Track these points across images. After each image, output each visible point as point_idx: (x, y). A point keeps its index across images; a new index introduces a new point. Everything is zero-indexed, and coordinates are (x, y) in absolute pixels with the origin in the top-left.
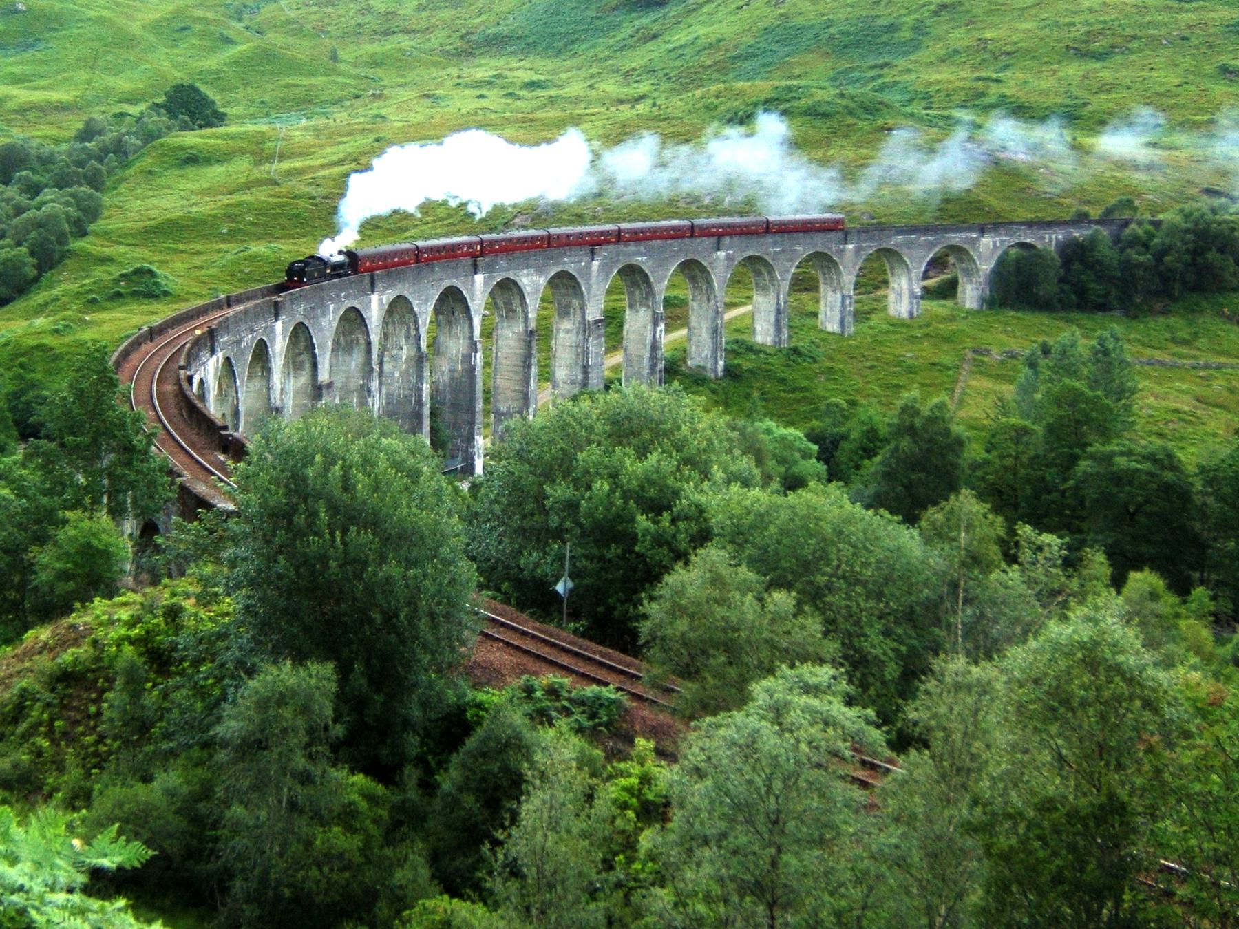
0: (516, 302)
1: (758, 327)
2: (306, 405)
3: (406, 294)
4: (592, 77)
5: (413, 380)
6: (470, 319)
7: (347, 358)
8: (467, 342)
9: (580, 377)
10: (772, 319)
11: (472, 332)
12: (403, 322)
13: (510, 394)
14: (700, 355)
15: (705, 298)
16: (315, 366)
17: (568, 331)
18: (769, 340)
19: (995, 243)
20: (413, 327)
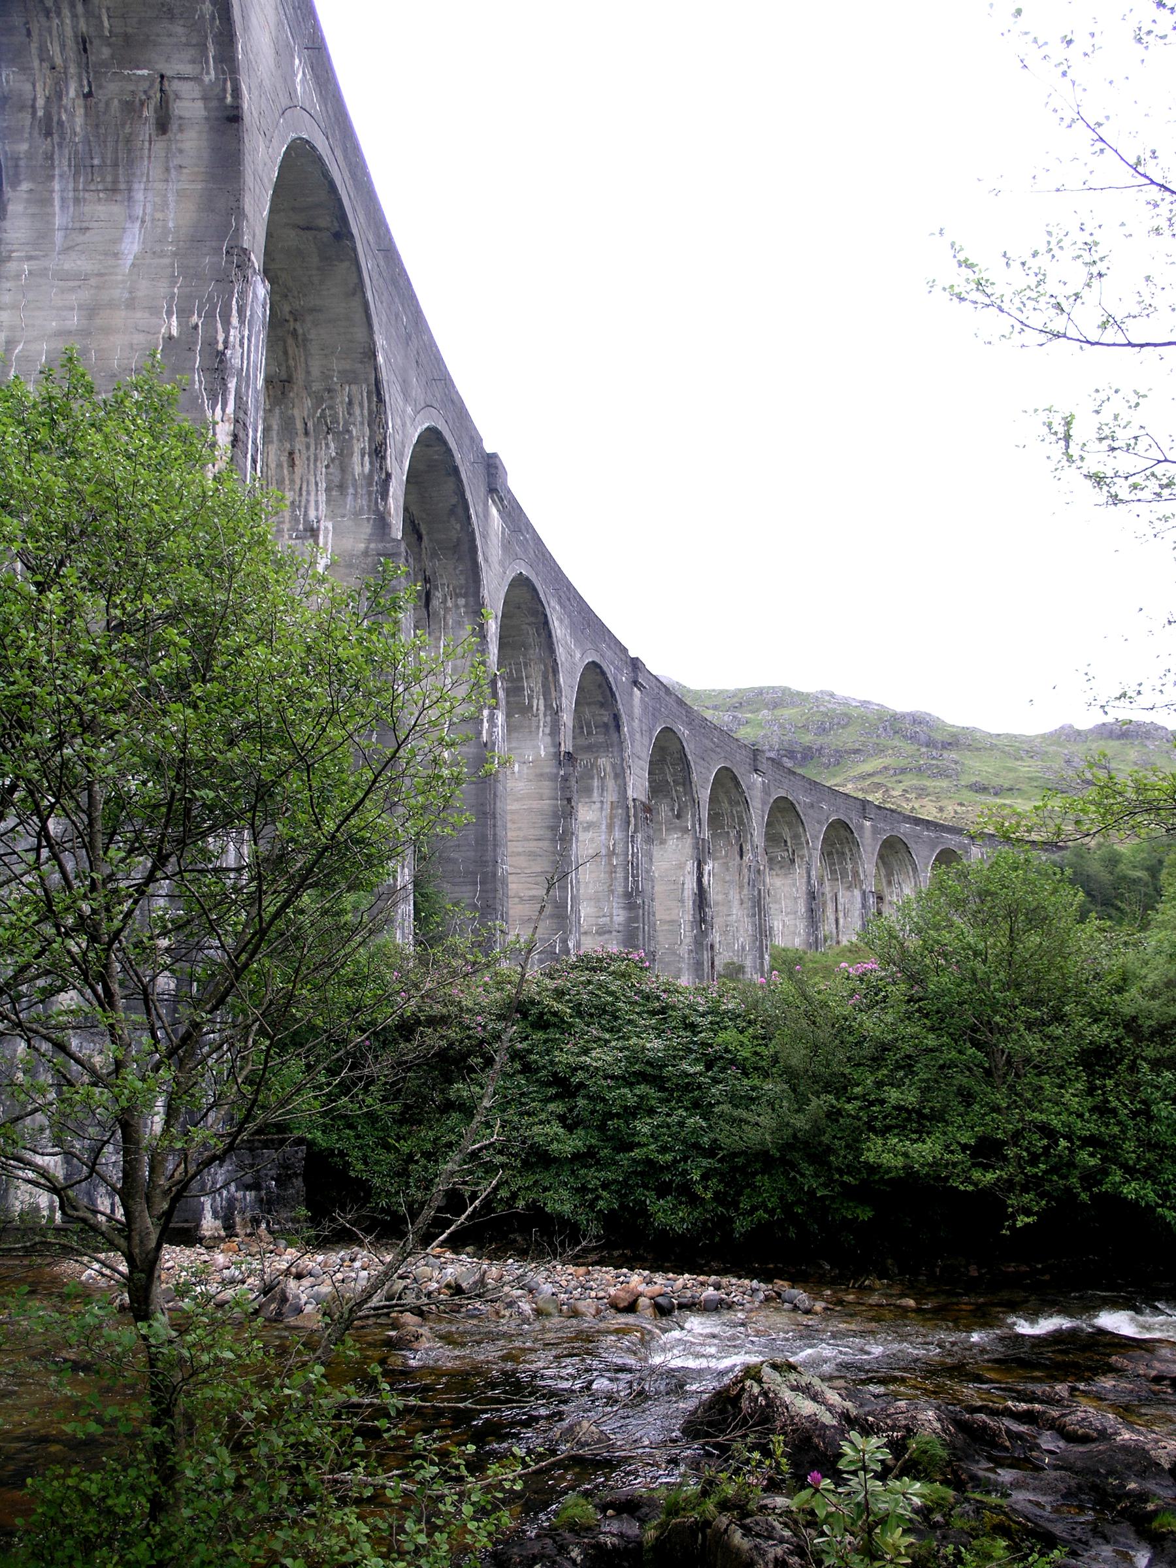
1: (777, 925)
7: (100, 210)
10: (802, 908)
12: (328, 427)
14: (729, 946)
17: (590, 826)
18: (798, 942)
20: (360, 444)
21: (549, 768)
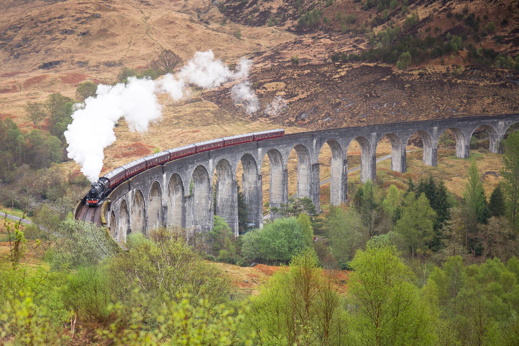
0: (279, 158)
2: (180, 205)
3: (226, 158)
4: (356, 41)
5: (230, 193)
6: (257, 167)
7: (201, 185)
8: (255, 175)
9: (309, 188)
11: (257, 172)
13: (277, 196)
15: (368, 152)
16: (183, 189)
17: (304, 169)
19: (505, 124)
21: (282, 172)
